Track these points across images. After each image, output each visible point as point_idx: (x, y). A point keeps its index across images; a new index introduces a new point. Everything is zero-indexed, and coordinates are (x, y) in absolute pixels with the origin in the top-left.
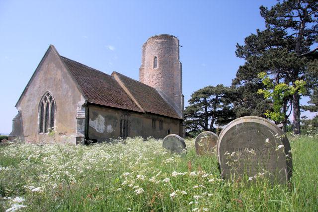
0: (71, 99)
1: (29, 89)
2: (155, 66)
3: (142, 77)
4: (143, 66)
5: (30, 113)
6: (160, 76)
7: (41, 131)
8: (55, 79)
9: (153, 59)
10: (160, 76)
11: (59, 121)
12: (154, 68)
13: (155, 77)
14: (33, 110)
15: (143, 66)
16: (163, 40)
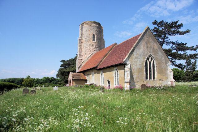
0: (164, 62)
1: (135, 50)
2: (94, 40)
3: (81, 45)
4: (81, 37)
5: (138, 66)
6: (97, 46)
7: (147, 78)
8: (153, 48)
9: (92, 35)
10: (97, 46)
11: (159, 73)
12: (93, 41)
13: (94, 47)
14: (140, 65)
15: (81, 37)
16: (98, 26)
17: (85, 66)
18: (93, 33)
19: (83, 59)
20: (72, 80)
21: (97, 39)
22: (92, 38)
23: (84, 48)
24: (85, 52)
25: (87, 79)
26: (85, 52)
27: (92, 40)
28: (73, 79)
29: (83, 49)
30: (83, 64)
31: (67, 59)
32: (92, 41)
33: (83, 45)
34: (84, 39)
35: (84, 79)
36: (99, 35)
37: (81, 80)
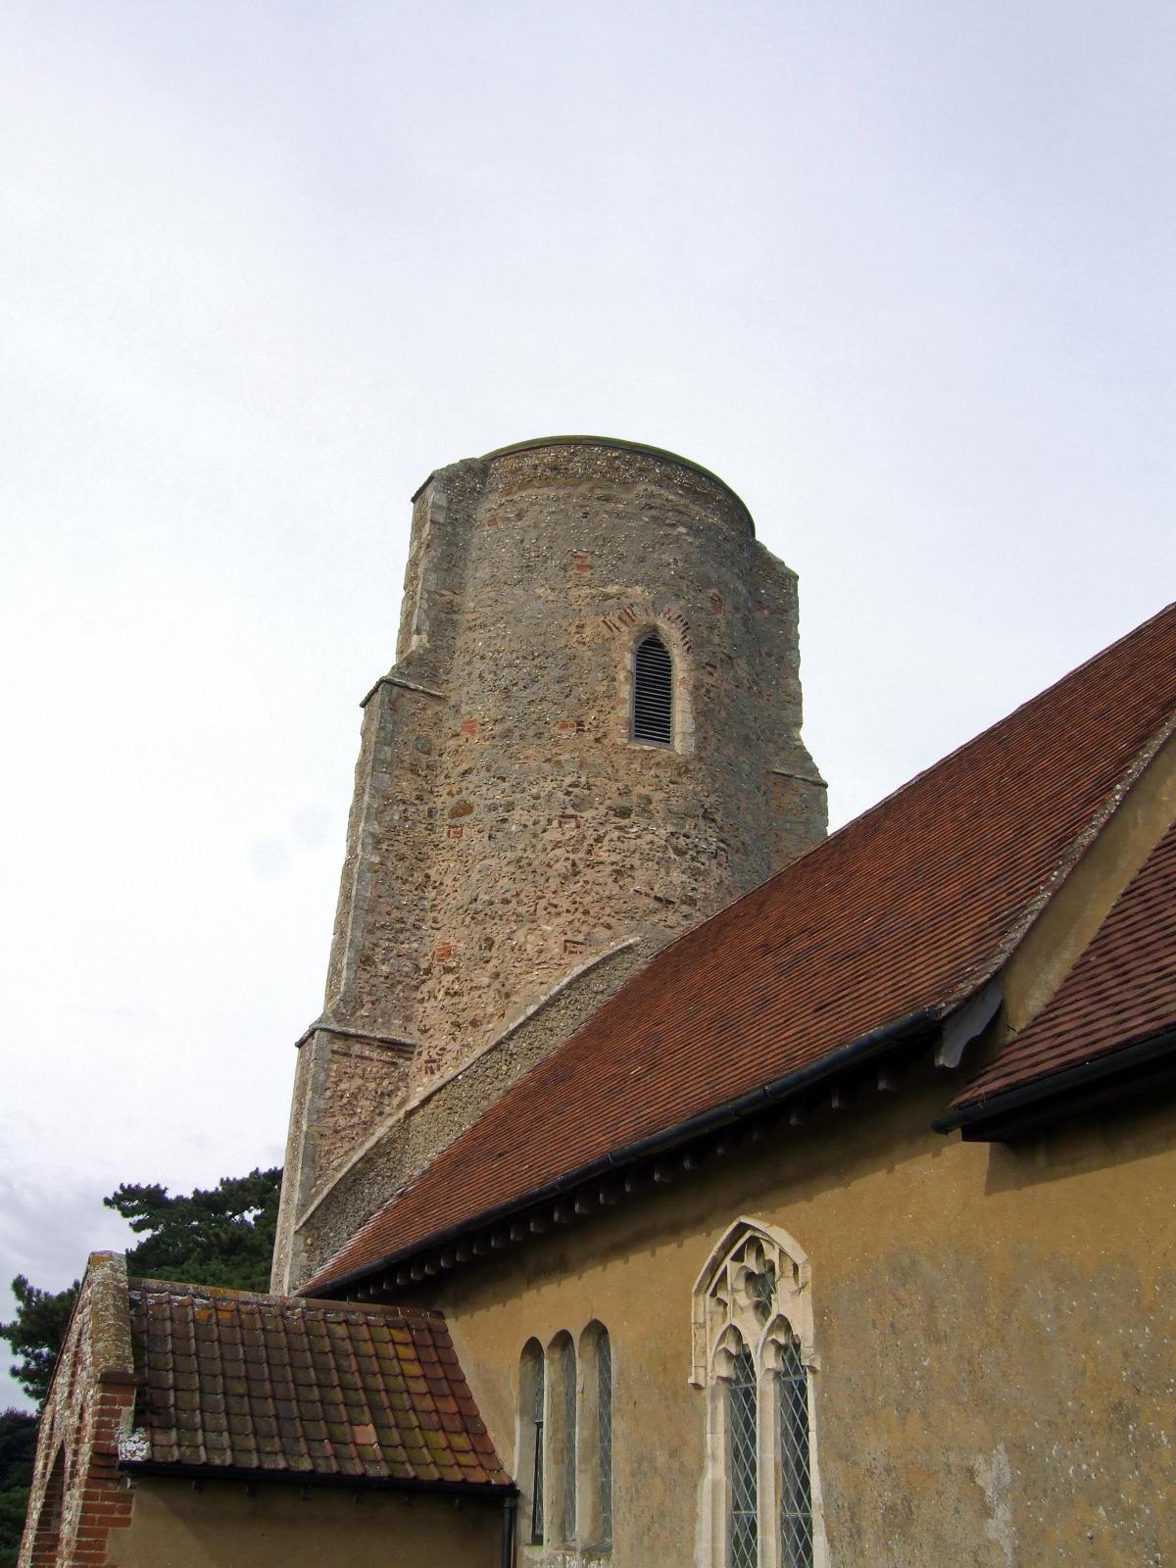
2: (651, 720)
3: (407, 787)
17: (454, 1165)
18: (643, 619)
19: (427, 1046)
20: (105, 1460)
21: (703, 714)
22: (626, 691)
23: (480, 844)
24: (475, 913)
25: (514, 1465)
26: (475, 913)
27: (626, 711)
28: (133, 1447)
29: (443, 867)
30: (424, 1154)
31: (188, 1176)
32: (619, 735)
33: (444, 801)
34: (472, 697)
35: (437, 1459)
36: (742, 669)
37: (360, 1488)
